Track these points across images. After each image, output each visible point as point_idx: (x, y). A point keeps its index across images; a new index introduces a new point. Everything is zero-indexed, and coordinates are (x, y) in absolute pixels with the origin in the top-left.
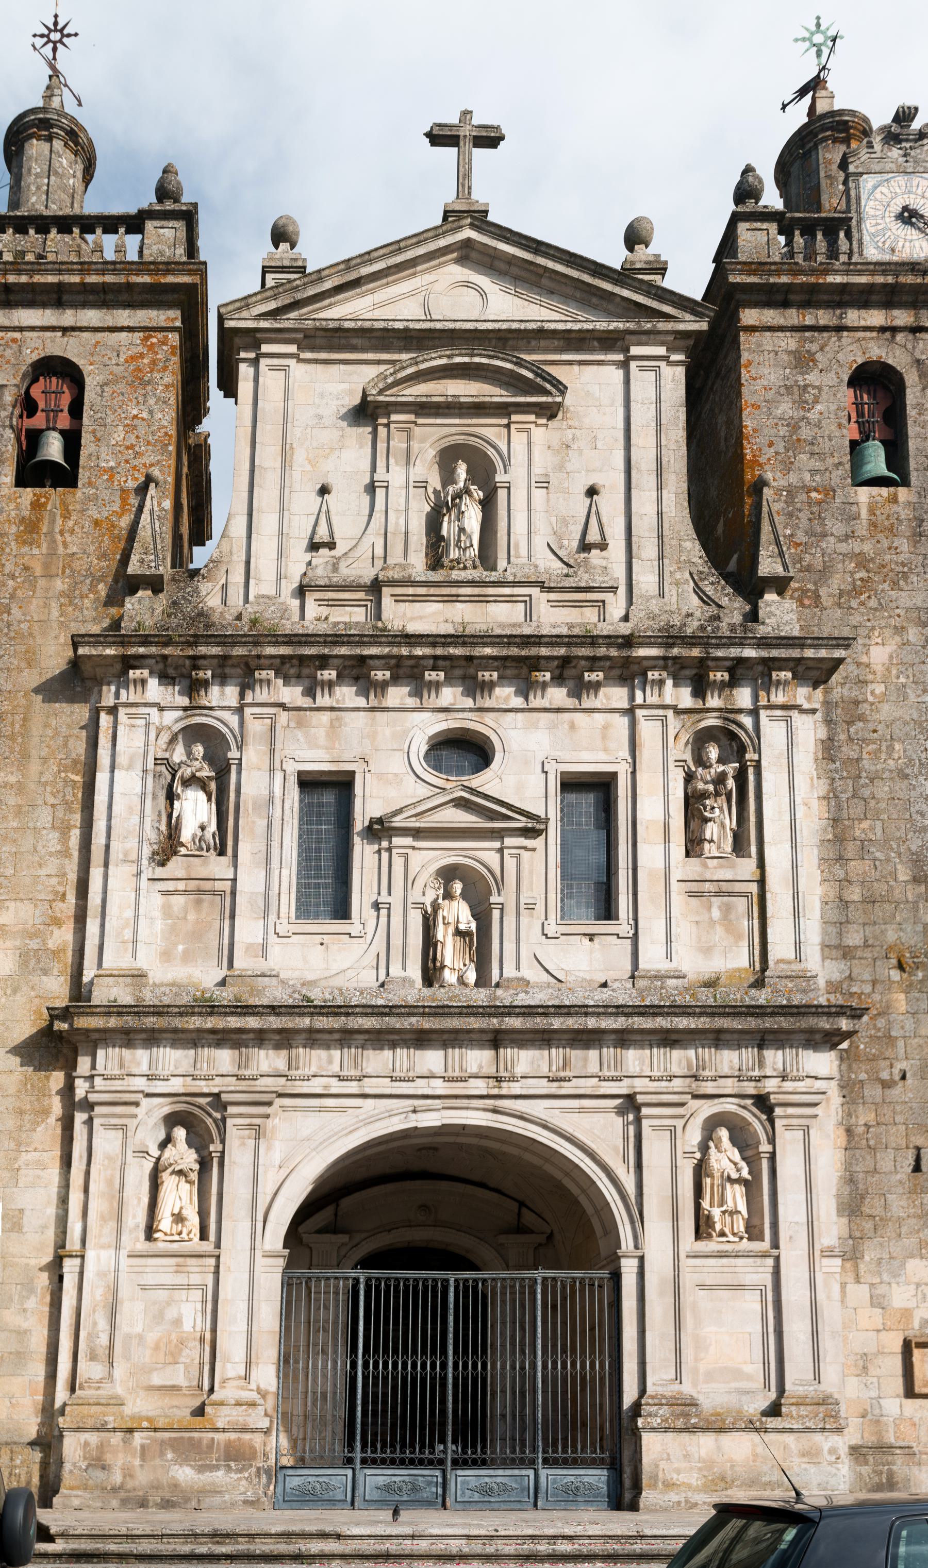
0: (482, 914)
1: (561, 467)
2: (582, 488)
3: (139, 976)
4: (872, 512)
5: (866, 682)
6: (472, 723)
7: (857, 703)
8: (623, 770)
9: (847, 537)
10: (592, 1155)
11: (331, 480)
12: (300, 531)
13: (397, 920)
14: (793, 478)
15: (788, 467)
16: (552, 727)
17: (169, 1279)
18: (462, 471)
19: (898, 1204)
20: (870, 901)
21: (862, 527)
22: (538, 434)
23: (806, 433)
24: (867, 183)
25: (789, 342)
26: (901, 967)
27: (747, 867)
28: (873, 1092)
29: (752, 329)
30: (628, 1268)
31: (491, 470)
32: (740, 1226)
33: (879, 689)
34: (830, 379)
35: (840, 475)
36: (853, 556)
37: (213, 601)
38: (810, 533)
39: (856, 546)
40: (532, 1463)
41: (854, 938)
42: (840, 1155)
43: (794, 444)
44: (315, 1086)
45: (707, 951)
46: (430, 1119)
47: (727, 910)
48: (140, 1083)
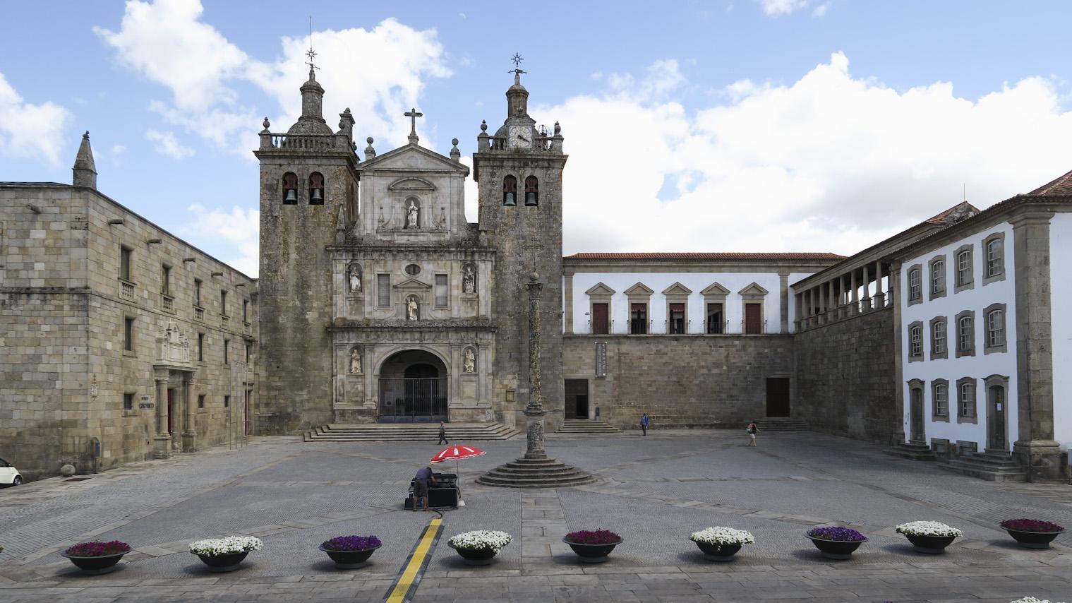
0: (418, 305)
1: (435, 203)
2: (440, 207)
3: (344, 319)
4: (507, 211)
5: (503, 252)
6: (416, 263)
7: (502, 257)
8: (449, 273)
9: (501, 218)
10: (442, 355)
11: (383, 206)
12: (377, 216)
13: (400, 306)
14: (490, 204)
15: (489, 201)
16: (433, 264)
17: (354, 380)
18: (412, 204)
19: (507, 364)
20: (503, 301)
21: (505, 216)
22: (430, 196)
23: (493, 192)
24: (511, 127)
25: (489, 170)
26: (509, 315)
27: (476, 294)
28: (502, 341)
29: (481, 167)
30: (449, 377)
31: (419, 204)
32: (472, 369)
33: (507, 254)
34: (499, 179)
35: (502, 203)
36: (503, 223)
37: (357, 234)
38: (493, 217)
39: (503, 220)
40: (430, 414)
41: (499, 309)
42: (494, 355)
43: (490, 196)
44: (383, 342)
45: (467, 313)
46: (408, 348)
47: (471, 304)
48: (346, 342)
